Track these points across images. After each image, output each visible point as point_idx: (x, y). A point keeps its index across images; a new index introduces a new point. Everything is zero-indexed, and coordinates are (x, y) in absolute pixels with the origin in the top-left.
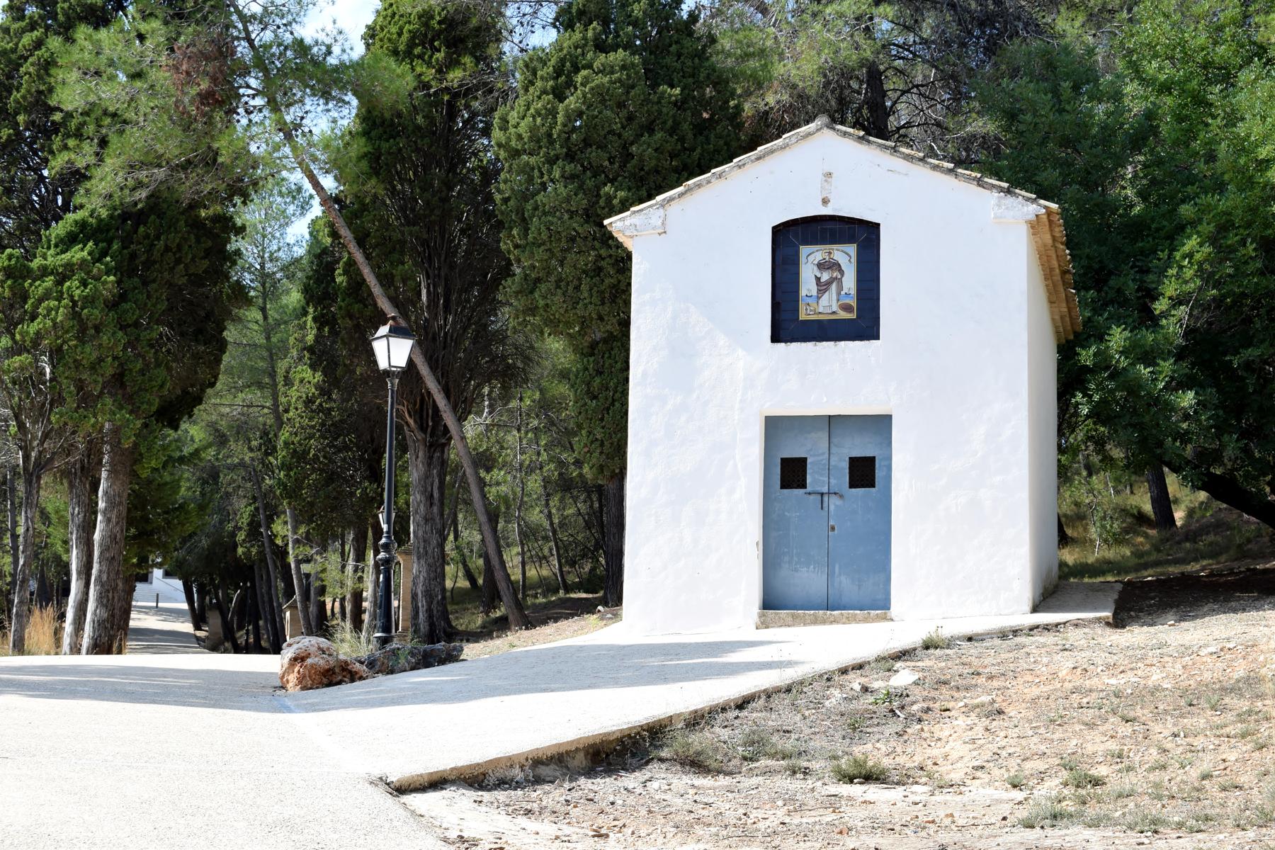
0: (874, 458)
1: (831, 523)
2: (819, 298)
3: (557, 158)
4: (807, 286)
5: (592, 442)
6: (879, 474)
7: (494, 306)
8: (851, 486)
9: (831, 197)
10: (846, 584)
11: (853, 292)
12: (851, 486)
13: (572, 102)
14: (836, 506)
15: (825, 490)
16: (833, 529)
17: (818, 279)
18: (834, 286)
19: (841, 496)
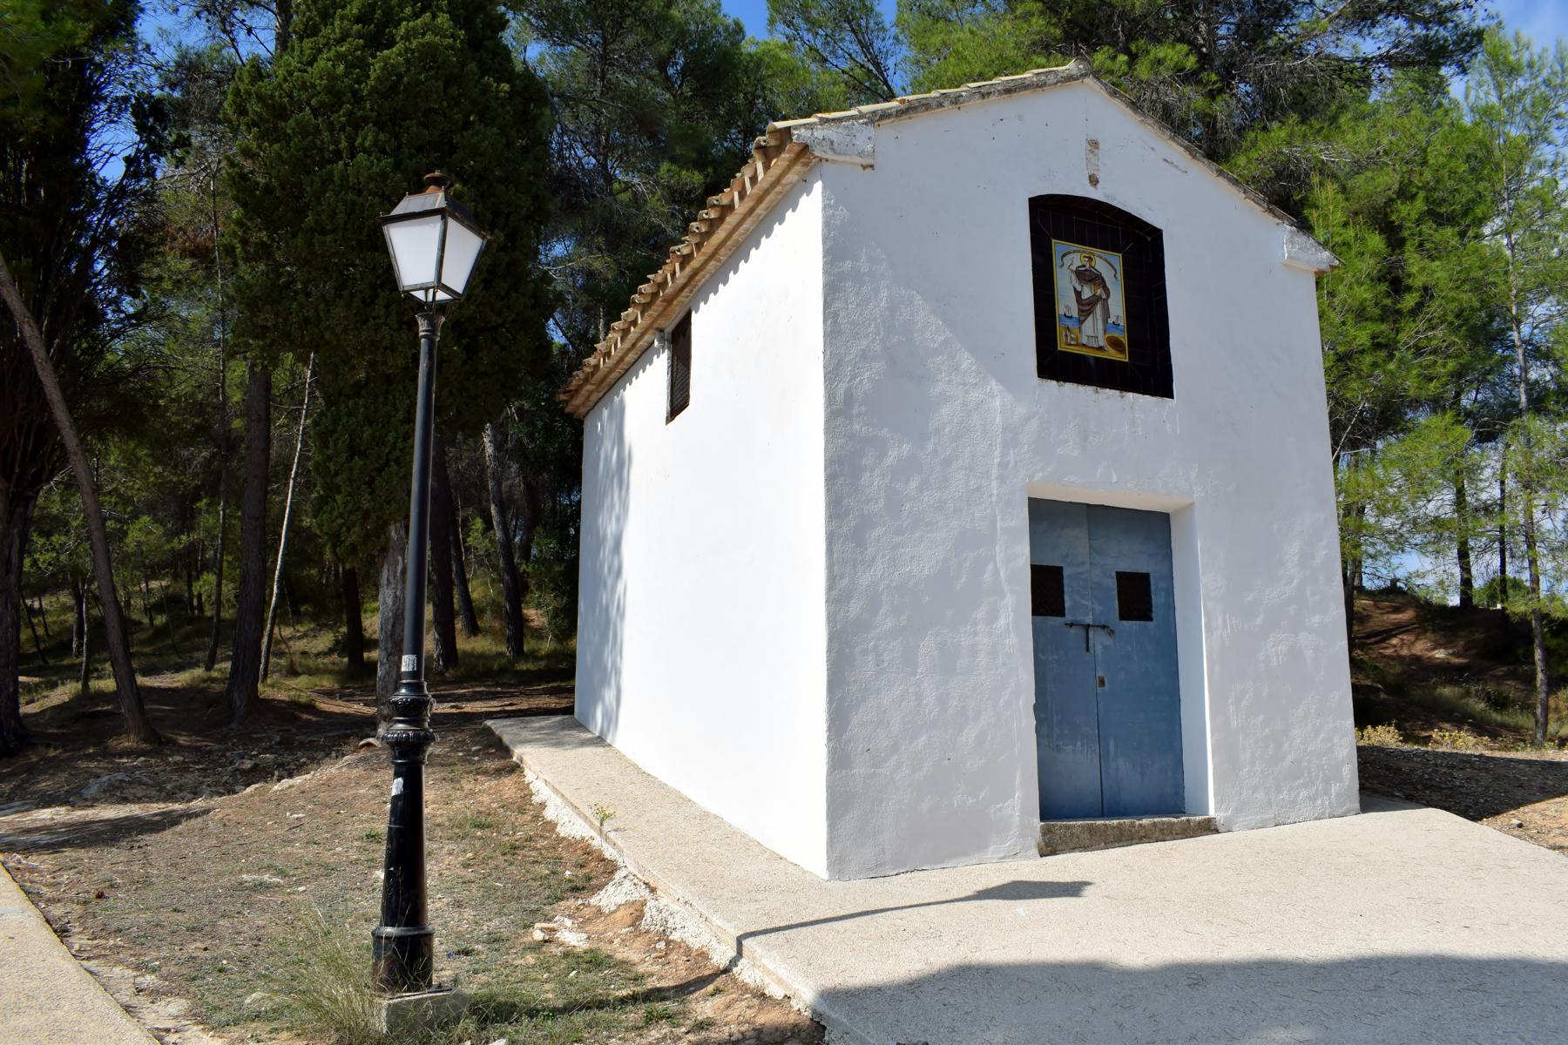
0: (1147, 575)
1: (1100, 673)
2: (1081, 322)
3: (365, 120)
4: (1066, 303)
5: (351, 512)
6: (1157, 600)
7: (583, 237)
8: (1123, 617)
9: (1100, 176)
10: (1129, 776)
11: (1122, 322)
12: (1123, 617)
13: (392, 54)
14: (1105, 647)
15: (1089, 620)
16: (1102, 682)
17: (1078, 294)
18: (1098, 309)
19: (1112, 633)
